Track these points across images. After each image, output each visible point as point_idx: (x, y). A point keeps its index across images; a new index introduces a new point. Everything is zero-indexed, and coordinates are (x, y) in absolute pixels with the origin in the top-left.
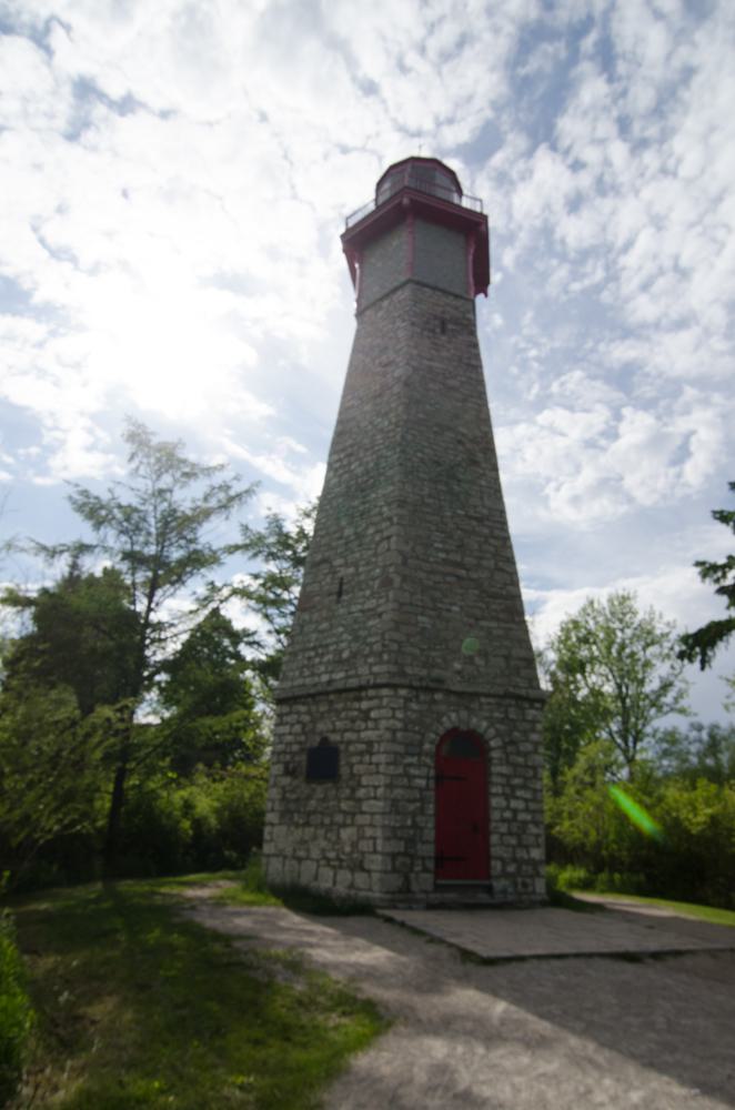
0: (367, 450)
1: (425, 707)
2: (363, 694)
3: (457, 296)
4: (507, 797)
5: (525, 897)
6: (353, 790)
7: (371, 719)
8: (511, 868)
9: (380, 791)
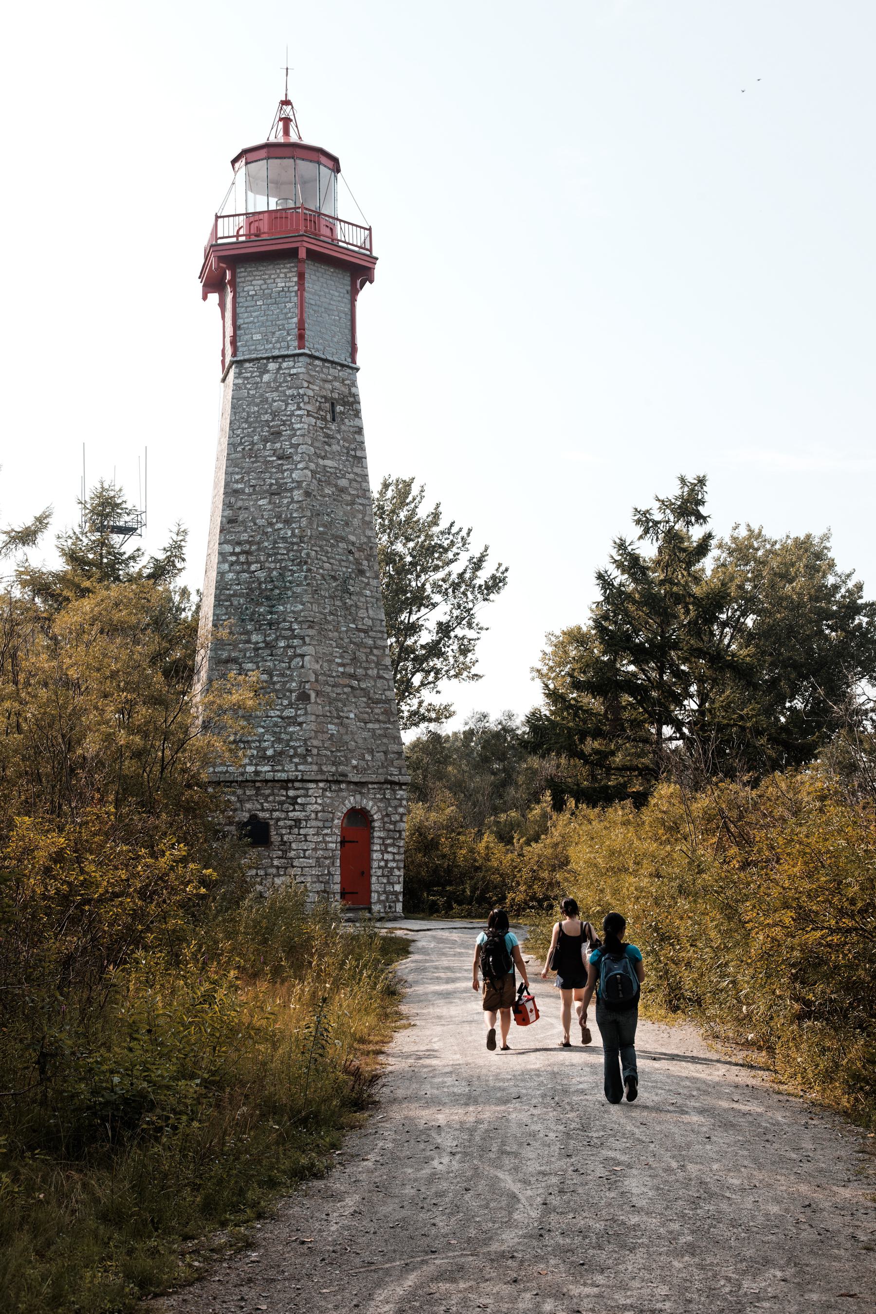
0: (269, 555)
1: (334, 795)
2: (290, 785)
3: (342, 366)
4: (383, 852)
5: (390, 915)
6: (285, 852)
7: (298, 804)
8: (383, 898)
9: (307, 853)
